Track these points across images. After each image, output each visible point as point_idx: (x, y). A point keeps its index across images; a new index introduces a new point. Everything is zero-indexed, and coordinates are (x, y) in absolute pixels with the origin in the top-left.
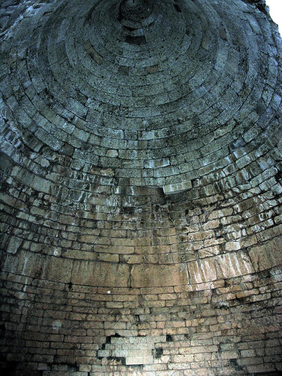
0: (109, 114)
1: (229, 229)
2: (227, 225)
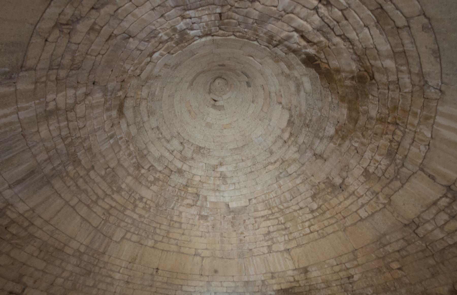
1: (274, 235)
2: (273, 232)
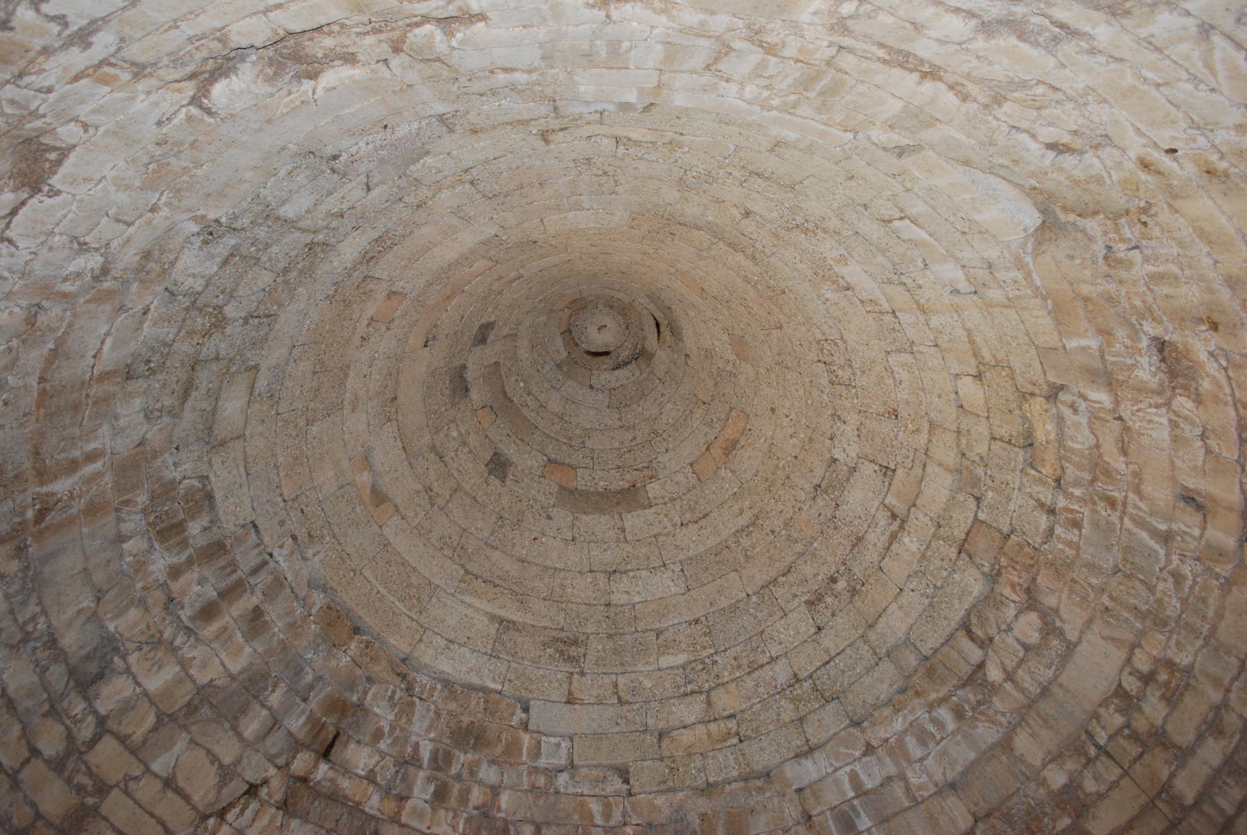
0: (856, 394)
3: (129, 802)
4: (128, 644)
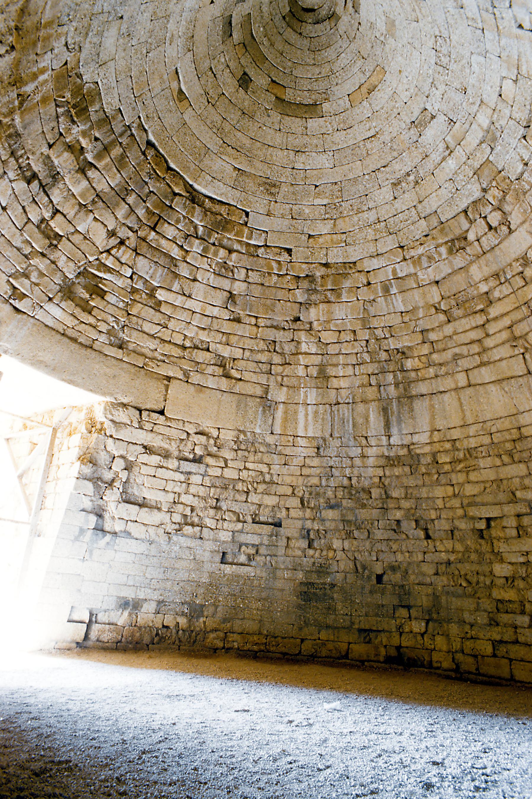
0: (448, 74)
3: (70, 243)
4: (64, 170)
